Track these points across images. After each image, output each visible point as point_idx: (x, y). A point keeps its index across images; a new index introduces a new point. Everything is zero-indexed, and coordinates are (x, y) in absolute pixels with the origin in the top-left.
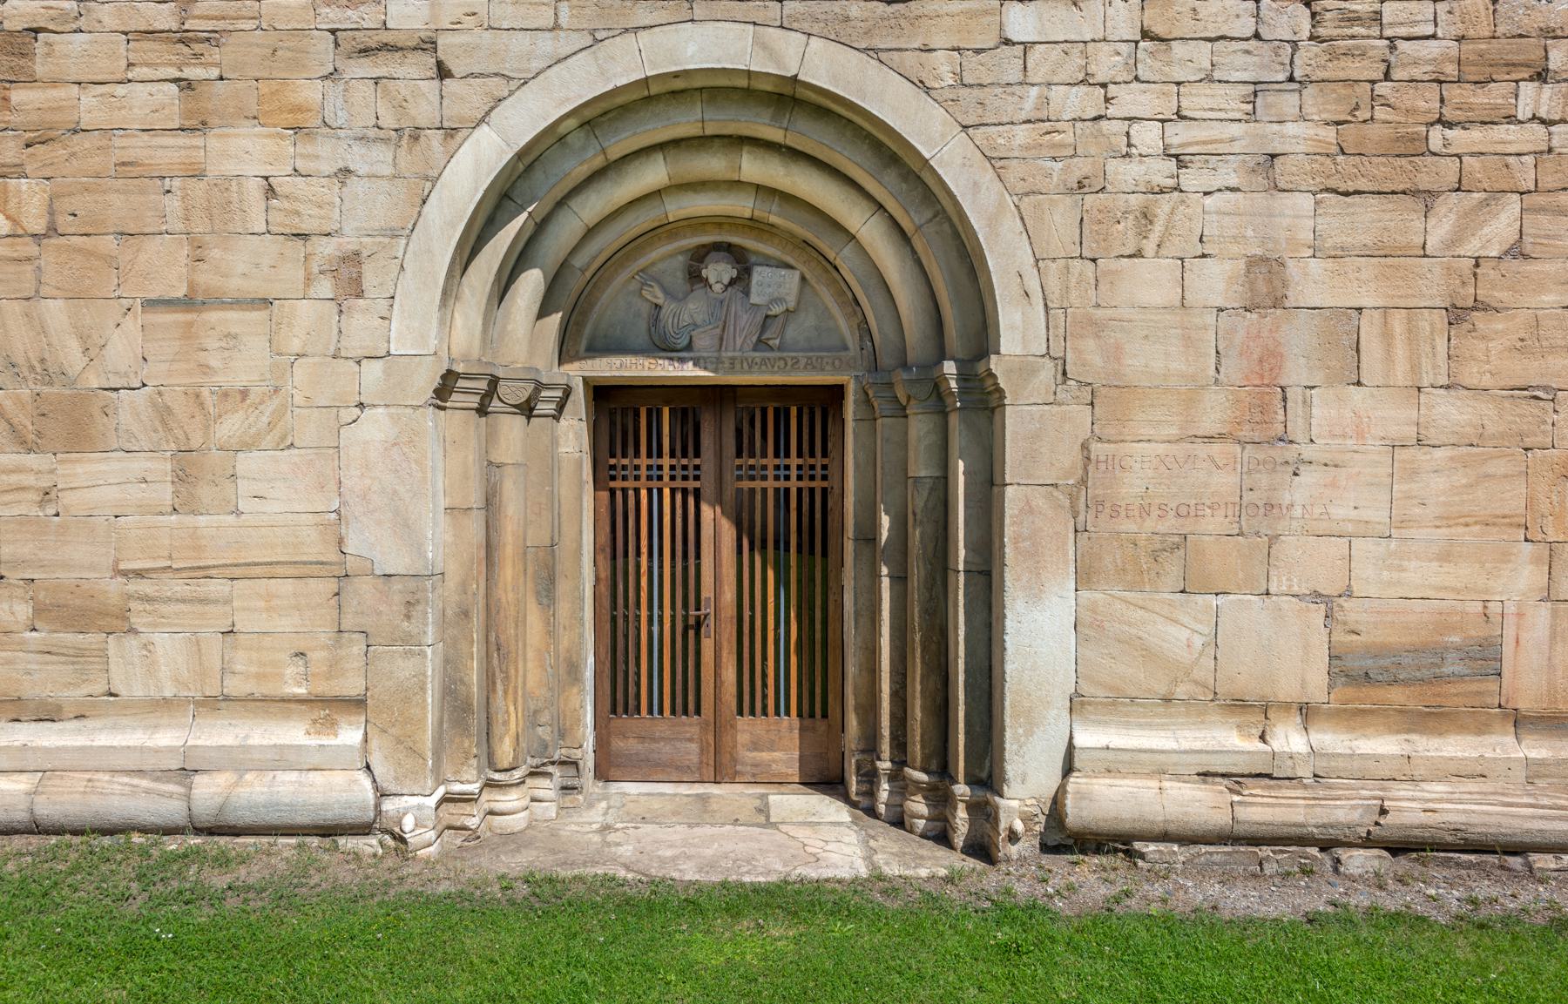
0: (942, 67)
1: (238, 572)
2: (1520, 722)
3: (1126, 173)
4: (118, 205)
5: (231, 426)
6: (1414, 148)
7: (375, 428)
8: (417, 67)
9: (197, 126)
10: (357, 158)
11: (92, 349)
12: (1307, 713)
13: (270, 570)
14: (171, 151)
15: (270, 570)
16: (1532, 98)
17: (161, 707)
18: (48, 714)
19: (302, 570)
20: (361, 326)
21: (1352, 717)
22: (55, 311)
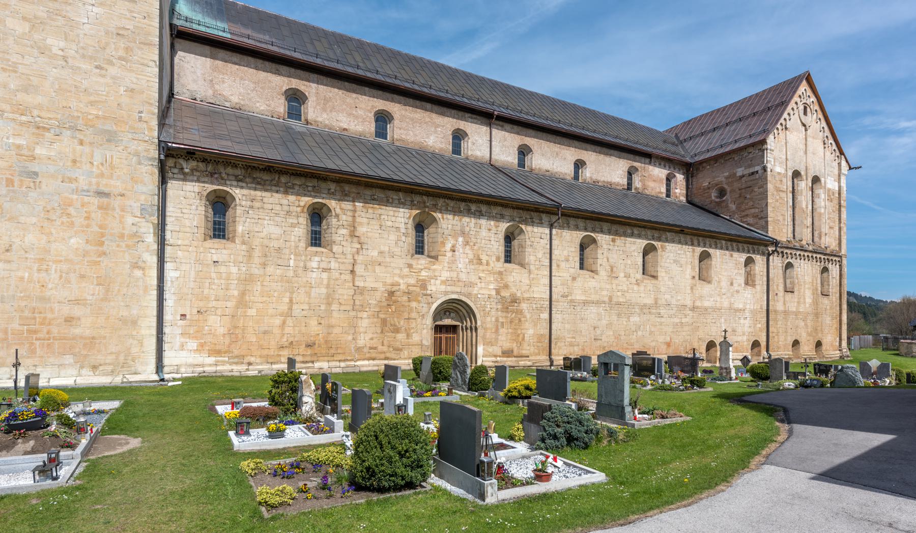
0: (473, 299)
1: (412, 345)
2: (515, 357)
3: (487, 309)
4: (402, 309)
5: (412, 331)
6: (507, 308)
7: (425, 331)
8: (429, 297)
9: (409, 301)
10: (424, 305)
11: (399, 323)
12: (500, 356)
13: (415, 345)
14: (407, 304)
15: (415, 345)
16: (516, 304)
17: (405, 359)
18: (394, 360)
19: (418, 345)
20: (424, 322)
21: (503, 357)
22: (395, 319)
